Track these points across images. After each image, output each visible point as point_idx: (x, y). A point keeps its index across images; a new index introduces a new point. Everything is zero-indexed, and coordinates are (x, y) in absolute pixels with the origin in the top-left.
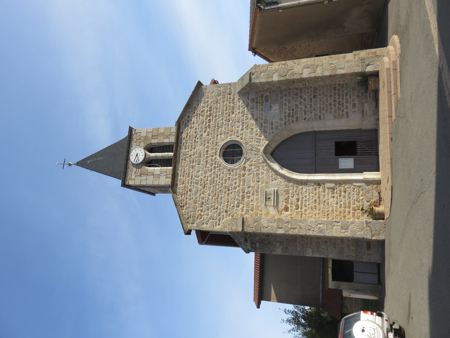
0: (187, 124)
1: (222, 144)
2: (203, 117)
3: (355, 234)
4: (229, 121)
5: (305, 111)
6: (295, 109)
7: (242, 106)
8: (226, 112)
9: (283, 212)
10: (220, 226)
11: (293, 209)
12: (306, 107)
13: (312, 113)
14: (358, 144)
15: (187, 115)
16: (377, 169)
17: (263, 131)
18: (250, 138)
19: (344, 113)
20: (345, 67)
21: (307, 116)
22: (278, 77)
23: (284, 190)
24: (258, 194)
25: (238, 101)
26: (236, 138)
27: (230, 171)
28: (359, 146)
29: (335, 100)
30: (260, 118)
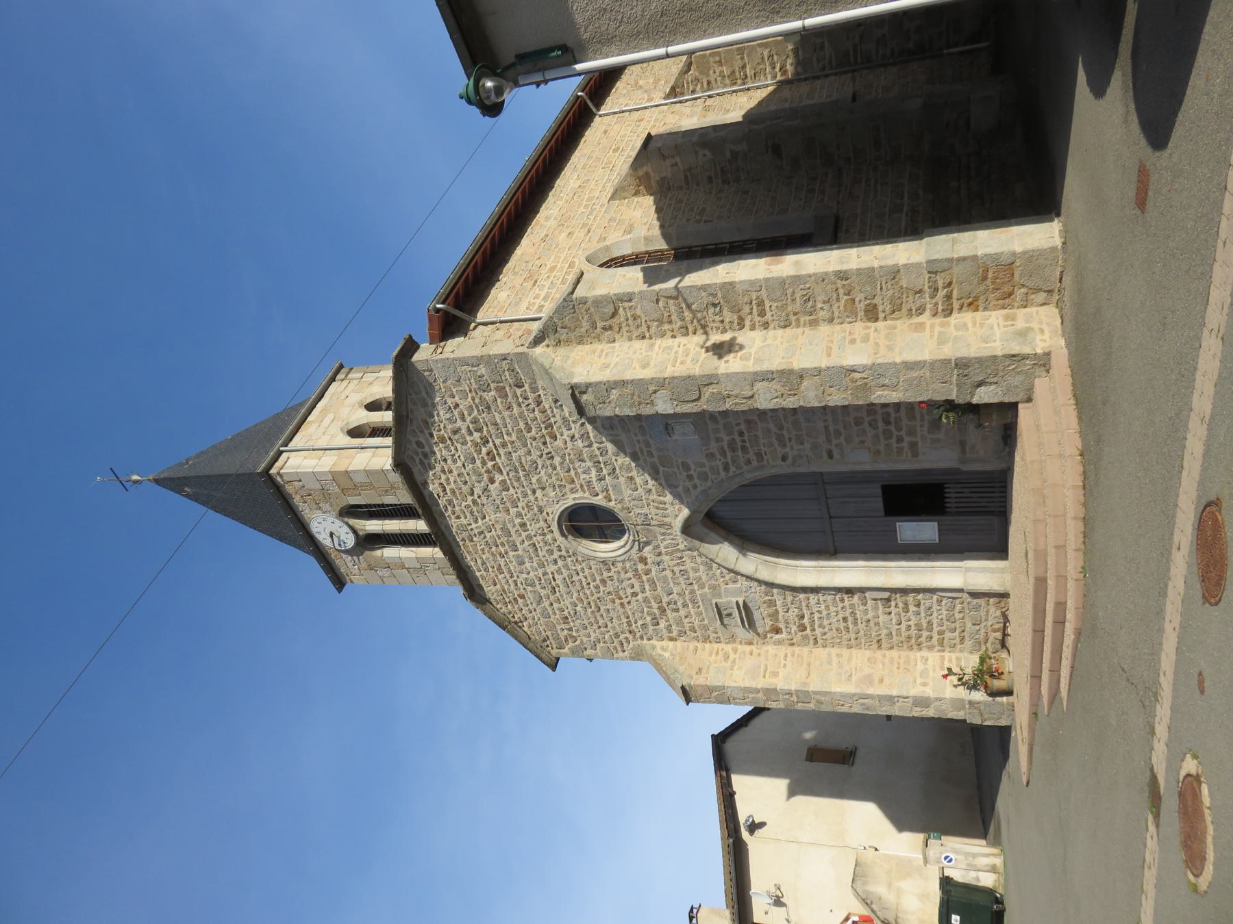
0: (426, 462)
1: (557, 510)
2: (464, 447)
3: (946, 715)
4: (552, 458)
5: (780, 439)
6: (748, 432)
7: (573, 422)
8: (529, 435)
9: (769, 635)
10: (626, 653)
11: (793, 631)
12: (781, 428)
13: (802, 444)
14: (949, 503)
15: (413, 440)
16: (999, 549)
17: (663, 482)
18: (634, 500)
19: (905, 444)
20: (901, 384)
21: (788, 450)
22: (673, 404)
23: (763, 600)
24: (697, 605)
25: (557, 408)
26: (590, 499)
27: (606, 565)
28: (951, 492)
29: (872, 409)
30: (645, 454)
